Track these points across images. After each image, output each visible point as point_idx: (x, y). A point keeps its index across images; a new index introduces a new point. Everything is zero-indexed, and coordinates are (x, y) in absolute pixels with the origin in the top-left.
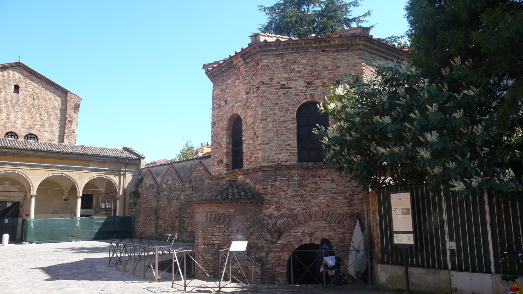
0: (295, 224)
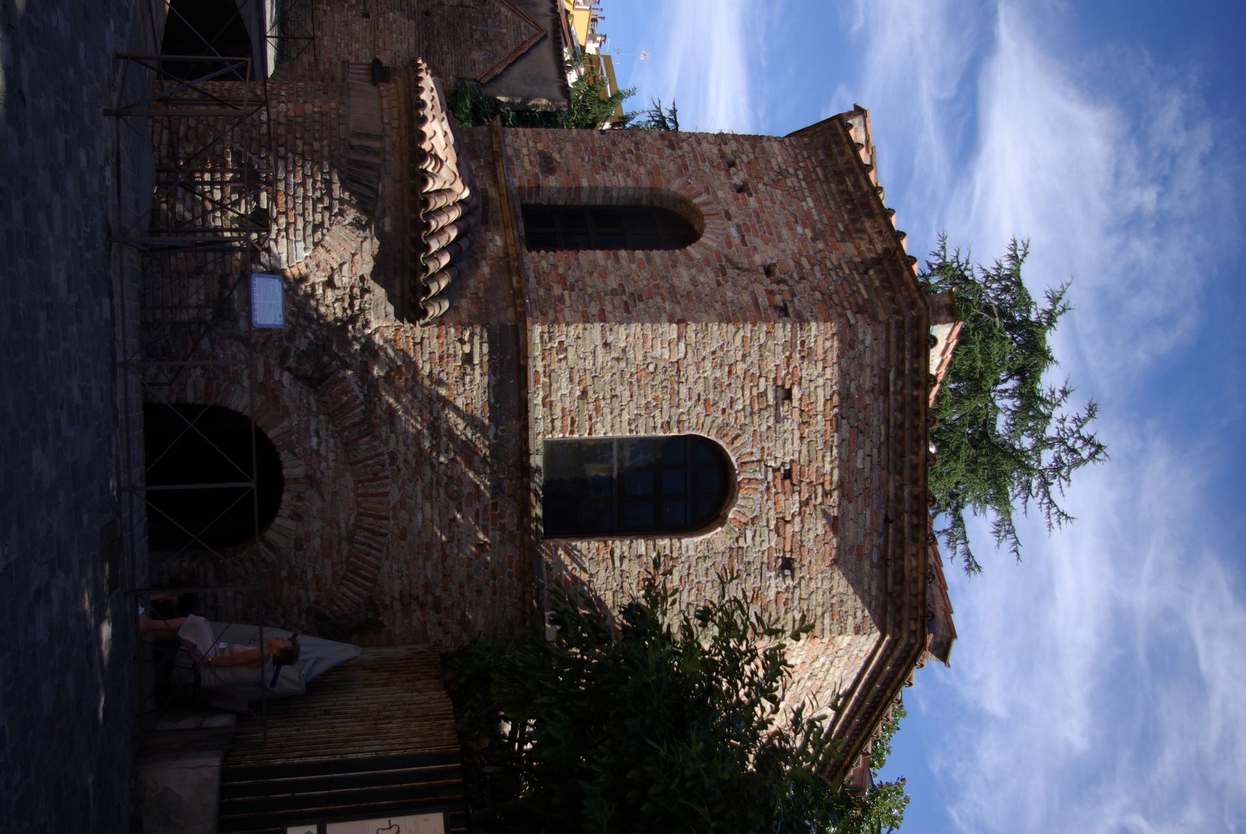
0: (345, 429)
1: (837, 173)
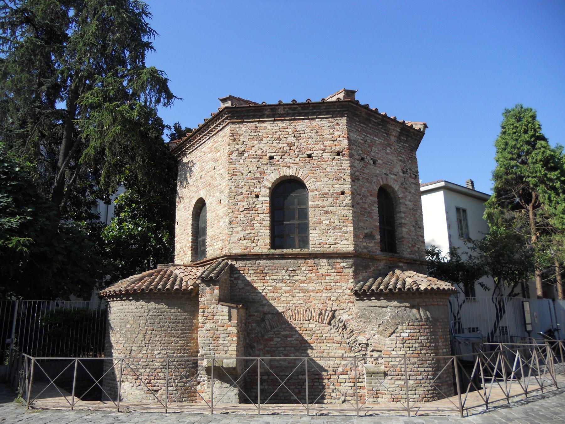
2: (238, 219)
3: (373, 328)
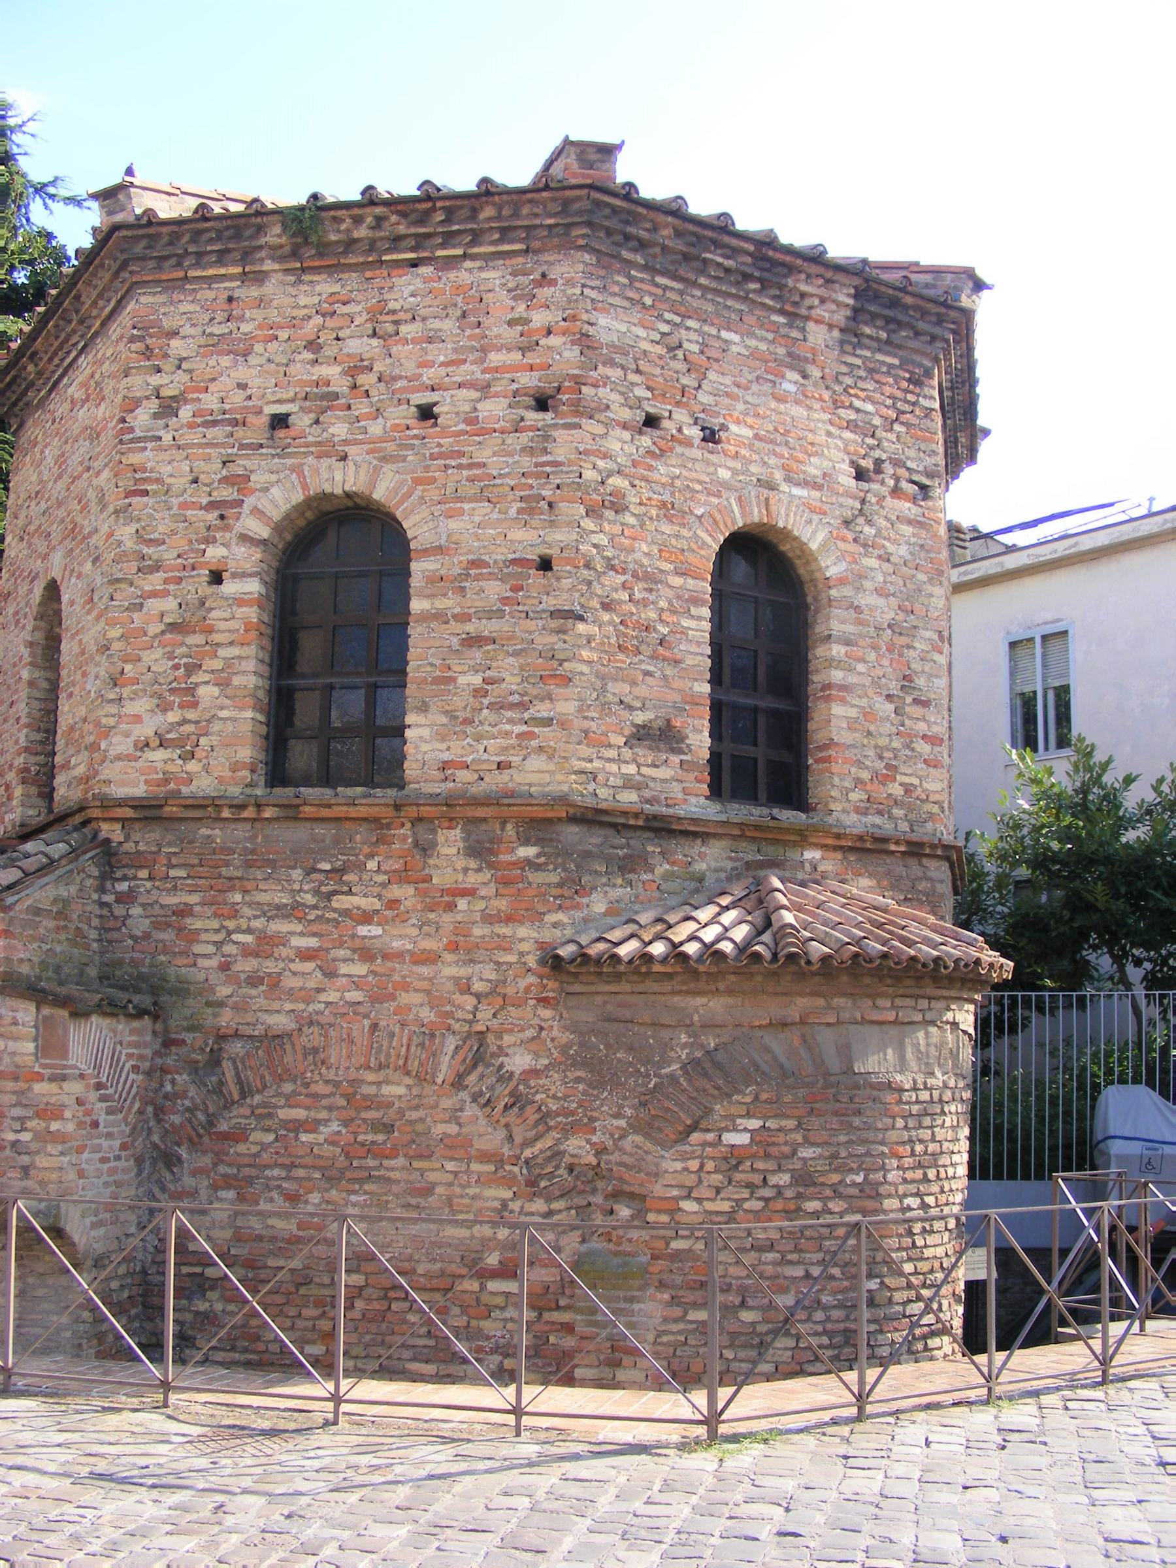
1: (686, 257)
2: (141, 667)
3: (622, 1107)
